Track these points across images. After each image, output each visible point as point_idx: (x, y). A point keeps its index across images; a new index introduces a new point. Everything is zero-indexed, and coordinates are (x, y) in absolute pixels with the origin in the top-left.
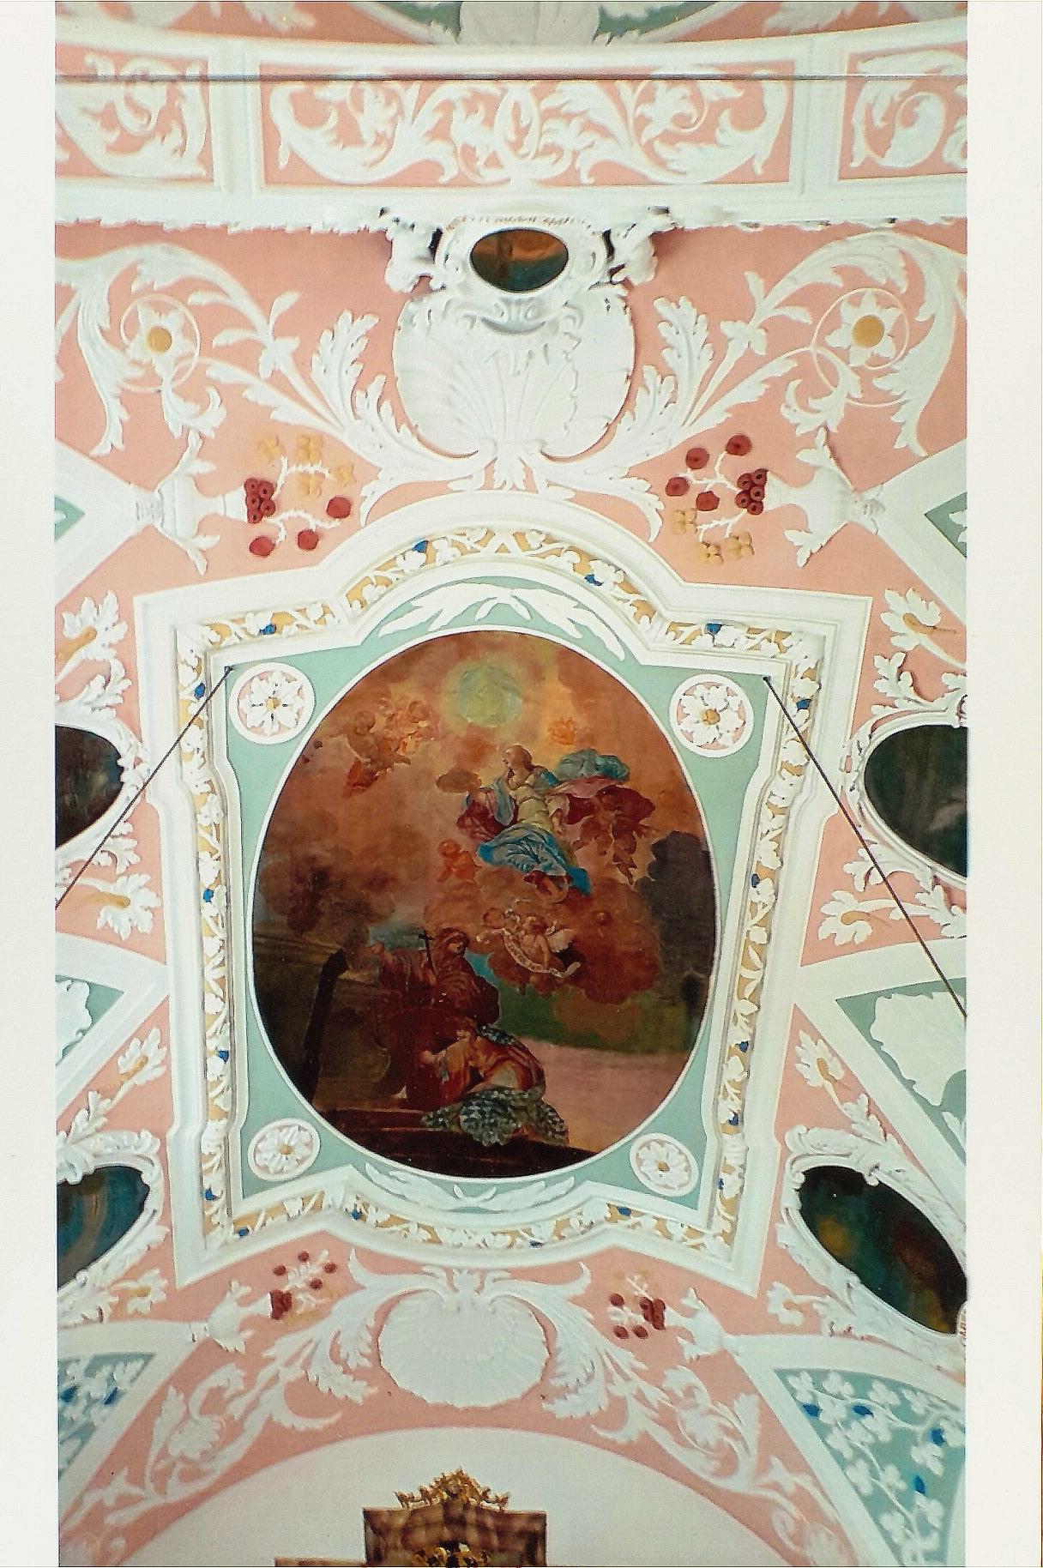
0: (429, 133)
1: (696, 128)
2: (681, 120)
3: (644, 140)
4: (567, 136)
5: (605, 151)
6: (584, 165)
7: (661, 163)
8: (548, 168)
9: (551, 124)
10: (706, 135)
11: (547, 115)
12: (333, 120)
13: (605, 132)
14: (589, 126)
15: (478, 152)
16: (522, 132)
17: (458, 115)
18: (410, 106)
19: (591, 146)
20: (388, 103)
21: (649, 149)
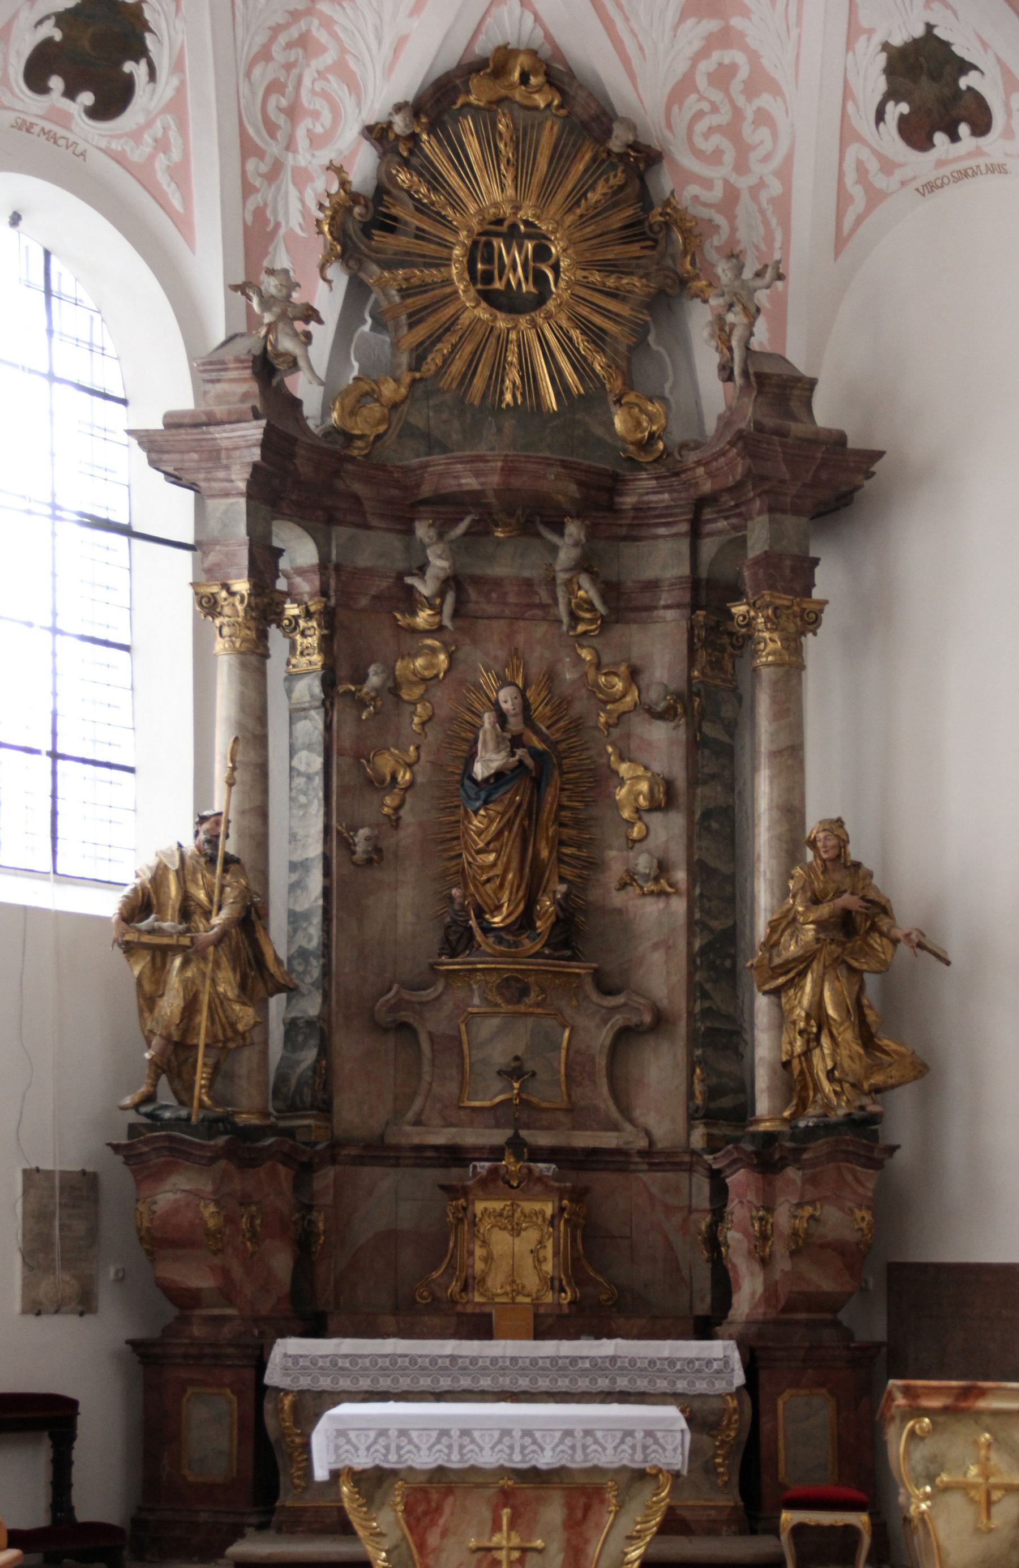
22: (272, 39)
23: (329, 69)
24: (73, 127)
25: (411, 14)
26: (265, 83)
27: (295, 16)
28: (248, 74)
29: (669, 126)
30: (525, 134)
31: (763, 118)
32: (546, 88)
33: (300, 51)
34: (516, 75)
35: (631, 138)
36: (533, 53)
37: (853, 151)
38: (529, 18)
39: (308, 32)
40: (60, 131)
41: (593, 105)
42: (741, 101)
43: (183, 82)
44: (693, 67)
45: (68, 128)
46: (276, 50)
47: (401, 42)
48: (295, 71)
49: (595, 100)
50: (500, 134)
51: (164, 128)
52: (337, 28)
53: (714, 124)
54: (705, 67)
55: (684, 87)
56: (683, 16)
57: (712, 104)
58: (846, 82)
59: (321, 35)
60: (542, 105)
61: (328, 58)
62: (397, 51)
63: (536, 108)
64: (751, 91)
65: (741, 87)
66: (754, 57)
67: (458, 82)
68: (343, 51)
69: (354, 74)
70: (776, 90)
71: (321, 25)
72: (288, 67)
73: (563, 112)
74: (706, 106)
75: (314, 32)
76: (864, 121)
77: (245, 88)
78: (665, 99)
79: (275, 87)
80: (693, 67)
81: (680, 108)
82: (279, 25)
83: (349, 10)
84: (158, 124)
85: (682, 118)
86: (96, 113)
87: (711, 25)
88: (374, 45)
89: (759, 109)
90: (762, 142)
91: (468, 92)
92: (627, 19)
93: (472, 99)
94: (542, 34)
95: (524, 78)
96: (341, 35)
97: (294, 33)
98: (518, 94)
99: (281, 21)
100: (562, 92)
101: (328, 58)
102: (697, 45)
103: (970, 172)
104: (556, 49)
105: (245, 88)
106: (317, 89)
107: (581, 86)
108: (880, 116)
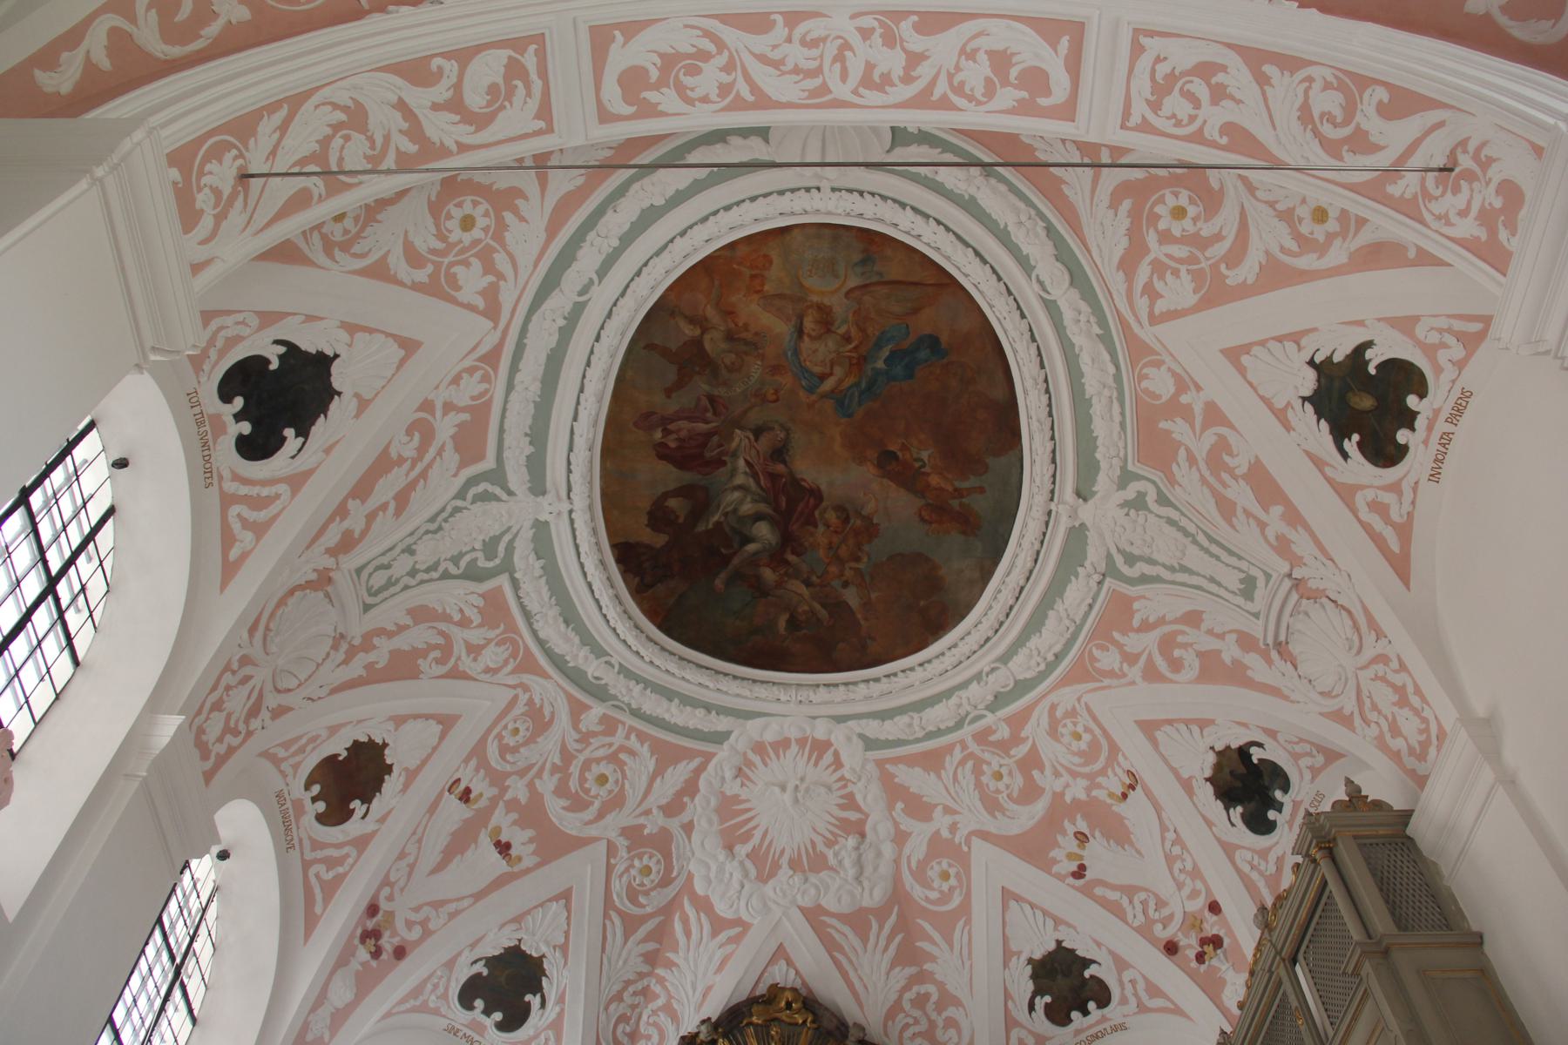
0: (928, 57)
1: (677, 68)
2: (694, 71)
3: (726, 53)
4: (796, 55)
5: (760, 43)
6: (780, 31)
7: (708, 34)
8: (813, 27)
9: (813, 65)
10: (669, 61)
11: (818, 72)
12: (1014, 72)
13: (762, 58)
14: (776, 64)
15: (880, 41)
16: (840, 58)
17: (898, 72)
18: (943, 78)
19: (774, 47)
20: (962, 84)
21: (721, 45)
22: (624, 989)
23: (660, 1009)
24: (486, 1035)
25: (715, 973)
26: (618, 1015)
27: (641, 976)
28: (606, 1009)
29: (886, 1035)
30: (789, 1038)
31: (951, 1023)
32: (803, 1010)
33: (642, 999)
34: (783, 1004)
35: (862, 1035)
36: (794, 990)
37: (1015, 1033)
38: (792, 973)
39: (648, 986)
40: (477, 1037)
41: (834, 1020)
42: (934, 1016)
43: (562, 1010)
44: (900, 998)
45: (482, 1036)
46: (626, 995)
47: (709, 988)
48: (638, 1010)
49: (835, 1016)
50: (772, 1037)
51: (546, 1039)
52: (667, 984)
53: (917, 1031)
54: (908, 996)
55: (894, 1010)
56: (892, 966)
57: (915, 1018)
58: (1006, 989)
59: (657, 989)
60: (800, 1021)
61: (660, 1002)
62: (705, 996)
63: (797, 1024)
64: (940, 1008)
65: (934, 1006)
66: (941, 986)
67: (744, 1009)
68: (670, 997)
69: (676, 1010)
70: (957, 1003)
71: (657, 982)
72: (633, 1007)
73: (815, 1026)
74: (911, 1021)
75: (652, 985)
76: (1021, 1013)
77: (603, 1017)
78: (883, 1019)
79: (623, 1019)
80: (900, 998)
81: (893, 1022)
82: (629, 980)
83: (676, 973)
84: (543, 1037)
85: (895, 1029)
86: (503, 1026)
87: (912, 970)
88: (690, 993)
89: (946, 1018)
90: (950, 1039)
91: (751, 1015)
92: (856, 970)
93: (754, 1019)
94: (800, 982)
95: (789, 1005)
96: (670, 988)
97: (639, 986)
98: (784, 1016)
99: (631, 978)
100: (814, 1014)
101: (660, 1002)
102: (902, 983)
103: (1099, 1034)
104: (810, 991)
105: (603, 1017)
106: (651, 1021)
107: (826, 1009)
108: (1031, 1007)
